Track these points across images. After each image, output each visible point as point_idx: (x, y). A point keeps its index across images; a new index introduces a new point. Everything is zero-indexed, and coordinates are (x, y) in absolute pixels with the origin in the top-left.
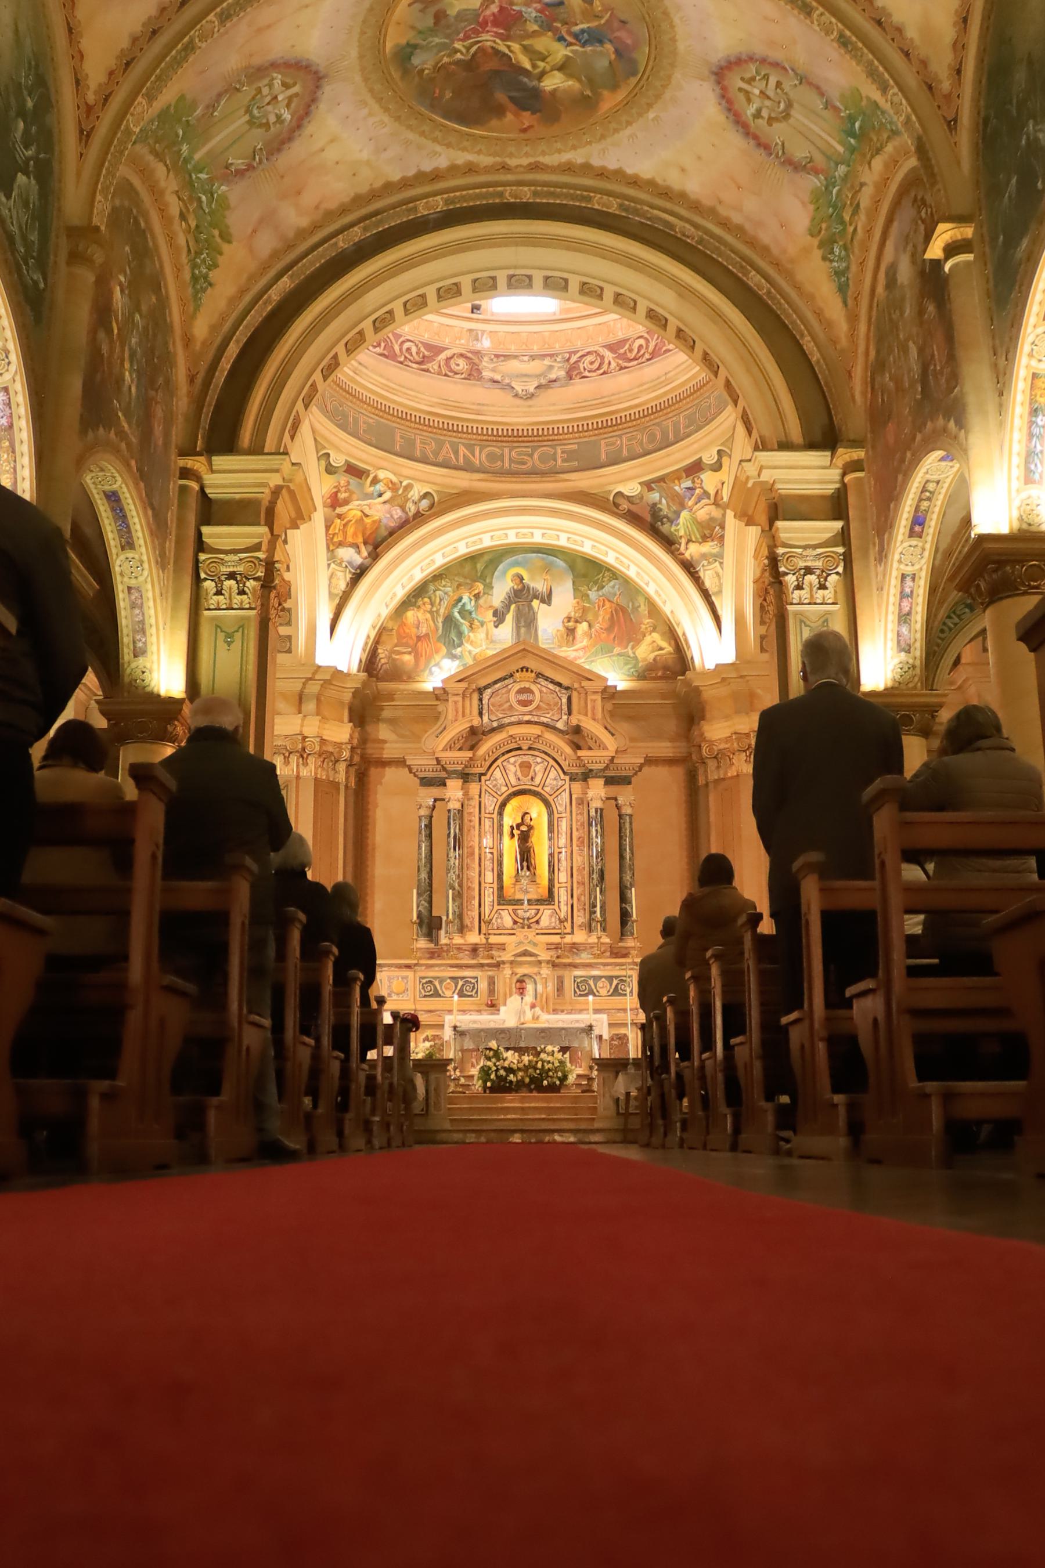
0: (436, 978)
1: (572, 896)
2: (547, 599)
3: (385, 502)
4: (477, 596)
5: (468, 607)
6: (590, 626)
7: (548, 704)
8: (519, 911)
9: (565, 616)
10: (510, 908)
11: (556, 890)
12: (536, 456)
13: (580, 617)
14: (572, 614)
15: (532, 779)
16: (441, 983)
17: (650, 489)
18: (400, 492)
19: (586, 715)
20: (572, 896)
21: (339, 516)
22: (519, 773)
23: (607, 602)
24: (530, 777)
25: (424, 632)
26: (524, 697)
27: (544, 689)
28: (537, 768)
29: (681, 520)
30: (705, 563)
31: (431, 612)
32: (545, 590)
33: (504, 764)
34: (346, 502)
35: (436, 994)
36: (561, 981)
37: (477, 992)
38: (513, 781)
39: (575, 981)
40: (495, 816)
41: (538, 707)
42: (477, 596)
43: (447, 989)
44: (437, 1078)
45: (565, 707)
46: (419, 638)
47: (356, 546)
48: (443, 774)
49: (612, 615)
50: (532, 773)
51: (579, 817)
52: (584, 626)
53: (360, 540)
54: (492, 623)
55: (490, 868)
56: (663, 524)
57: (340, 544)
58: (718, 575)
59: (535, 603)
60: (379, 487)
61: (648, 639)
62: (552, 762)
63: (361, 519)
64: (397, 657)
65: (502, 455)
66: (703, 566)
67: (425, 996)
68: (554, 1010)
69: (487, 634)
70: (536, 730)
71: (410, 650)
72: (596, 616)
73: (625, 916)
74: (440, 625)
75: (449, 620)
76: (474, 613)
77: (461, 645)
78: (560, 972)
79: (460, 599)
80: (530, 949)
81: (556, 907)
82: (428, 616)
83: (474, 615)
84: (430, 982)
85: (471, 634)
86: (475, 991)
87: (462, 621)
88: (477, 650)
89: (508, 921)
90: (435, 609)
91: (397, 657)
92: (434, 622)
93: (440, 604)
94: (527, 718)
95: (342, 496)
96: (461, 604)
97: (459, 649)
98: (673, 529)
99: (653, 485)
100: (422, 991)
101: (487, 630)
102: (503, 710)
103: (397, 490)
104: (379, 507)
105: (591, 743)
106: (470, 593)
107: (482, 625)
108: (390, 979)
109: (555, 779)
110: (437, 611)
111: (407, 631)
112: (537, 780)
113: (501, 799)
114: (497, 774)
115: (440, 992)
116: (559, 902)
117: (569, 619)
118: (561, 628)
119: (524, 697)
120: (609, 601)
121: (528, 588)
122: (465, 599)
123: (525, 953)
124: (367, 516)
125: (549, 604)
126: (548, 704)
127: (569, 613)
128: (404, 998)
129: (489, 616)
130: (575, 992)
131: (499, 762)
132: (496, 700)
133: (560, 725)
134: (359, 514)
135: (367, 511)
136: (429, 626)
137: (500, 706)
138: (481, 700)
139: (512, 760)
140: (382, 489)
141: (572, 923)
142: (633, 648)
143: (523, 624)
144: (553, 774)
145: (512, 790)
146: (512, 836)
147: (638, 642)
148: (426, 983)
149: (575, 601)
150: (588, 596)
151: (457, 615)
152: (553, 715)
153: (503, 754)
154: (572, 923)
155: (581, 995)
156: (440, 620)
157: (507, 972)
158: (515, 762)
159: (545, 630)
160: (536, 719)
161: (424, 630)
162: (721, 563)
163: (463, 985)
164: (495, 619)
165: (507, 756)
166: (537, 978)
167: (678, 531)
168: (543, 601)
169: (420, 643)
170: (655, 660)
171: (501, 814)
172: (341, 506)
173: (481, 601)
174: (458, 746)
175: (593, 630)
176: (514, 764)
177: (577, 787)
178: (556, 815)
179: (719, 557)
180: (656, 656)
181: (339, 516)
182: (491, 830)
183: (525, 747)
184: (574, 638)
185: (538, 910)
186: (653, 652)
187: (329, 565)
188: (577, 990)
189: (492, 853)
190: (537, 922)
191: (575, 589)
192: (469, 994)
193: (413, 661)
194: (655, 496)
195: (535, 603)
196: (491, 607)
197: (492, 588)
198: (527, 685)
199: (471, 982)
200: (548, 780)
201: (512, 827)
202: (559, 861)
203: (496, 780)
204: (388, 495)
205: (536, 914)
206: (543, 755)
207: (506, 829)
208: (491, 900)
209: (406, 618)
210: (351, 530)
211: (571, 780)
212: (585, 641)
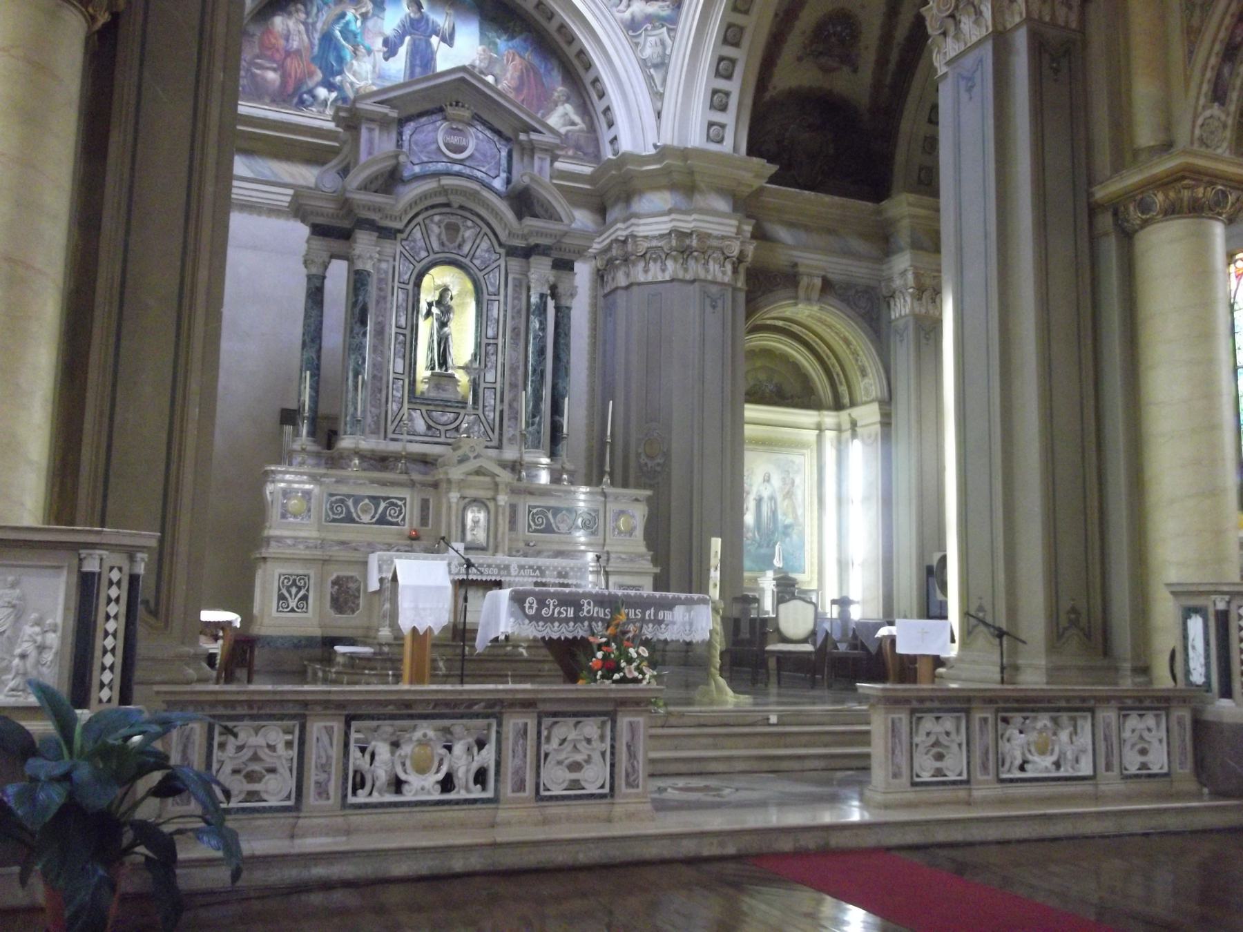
0: (349, 496)
1: (502, 401)
2: (449, 39)
4: (365, 17)
7: (485, 155)
8: (434, 413)
10: (424, 408)
11: (481, 391)
13: (487, 68)
14: (477, 63)
15: (460, 246)
16: (356, 503)
20: (502, 401)
22: (444, 237)
23: (517, 57)
24: (457, 244)
25: (295, 46)
27: (480, 135)
28: (468, 234)
30: (649, 26)
31: (305, 24)
32: (446, 26)
33: (427, 221)
35: (350, 519)
36: (513, 508)
37: (404, 519)
38: (436, 245)
39: (530, 512)
40: (410, 287)
41: (471, 157)
42: (365, 17)
43: (365, 511)
44: (631, 724)
45: (504, 162)
46: (288, 53)
48: (346, 224)
49: (522, 72)
50: (459, 239)
51: (516, 302)
54: (381, 54)
55: (401, 354)
58: (663, 43)
59: (435, 40)
61: (560, 110)
62: (486, 229)
64: (258, 72)
66: (646, 30)
67: (334, 520)
68: (510, 549)
71: (275, 66)
72: (505, 70)
73: (556, 429)
74: (316, 42)
75: (327, 38)
76: (359, 37)
77: (341, 72)
78: (515, 500)
79: (343, 15)
82: (302, 27)
83: (359, 39)
84: (342, 501)
85: (355, 62)
86: (401, 517)
87: (344, 42)
88: (362, 84)
89: (420, 425)
90: (310, 20)
91: (258, 72)
92: (308, 36)
93: (317, 15)
94: (457, 168)
96: (344, 21)
97: (338, 78)
100: (330, 513)
101: (375, 59)
102: (428, 152)
105: (538, 209)
106: (356, 10)
109: (488, 251)
110: (314, 24)
111: (273, 41)
112: (466, 248)
113: (419, 266)
114: (417, 234)
115: (354, 515)
116: (484, 407)
119: (455, 140)
120: (521, 57)
121: (427, 20)
122: (350, 15)
123: (479, 472)
125: (451, 45)
127: (474, 61)
128: (305, 521)
129: (378, 44)
130: (529, 526)
132: (419, 137)
136: (301, 40)
137: (425, 146)
138: (400, 134)
139: (437, 218)
141: (501, 434)
143: (418, 62)
145: (432, 257)
147: (549, 111)
148: (336, 502)
149: (480, 48)
150: (495, 44)
151: (338, 33)
152: (489, 169)
153: (427, 209)
154: (501, 434)
156: (317, 36)
157: (454, 496)
158: (440, 221)
160: (467, 171)
161: (295, 44)
162: (669, 30)
163: (386, 508)
164: (385, 49)
165: (431, 212)
166: (491, 505)
168: (443, 39)
169: (289, 60)
171: (418, 285)
173: (370, 24)
174: (374, 187)
176: (439, 224)
177: (515, 264)
179: (671, 22)
180: (568, 132)
182: (404, 305)
183: (456, 205)
185: (459, 414)
186: (565, 125)
188: (532, 523)
189: (404, 335)
192: (394, 520)
193: (278, 82)
195: (435, 40)
196: (381, 33)
197: (384, 10)
199: (396, 505)
200: (479, 250)
202: (486, 353)
203: (414, 241)
205: (456, 420)
206: (475, 218)
207: (423, 307)
208: (399, 395)
209: (272, 24)
211: (508, 254)
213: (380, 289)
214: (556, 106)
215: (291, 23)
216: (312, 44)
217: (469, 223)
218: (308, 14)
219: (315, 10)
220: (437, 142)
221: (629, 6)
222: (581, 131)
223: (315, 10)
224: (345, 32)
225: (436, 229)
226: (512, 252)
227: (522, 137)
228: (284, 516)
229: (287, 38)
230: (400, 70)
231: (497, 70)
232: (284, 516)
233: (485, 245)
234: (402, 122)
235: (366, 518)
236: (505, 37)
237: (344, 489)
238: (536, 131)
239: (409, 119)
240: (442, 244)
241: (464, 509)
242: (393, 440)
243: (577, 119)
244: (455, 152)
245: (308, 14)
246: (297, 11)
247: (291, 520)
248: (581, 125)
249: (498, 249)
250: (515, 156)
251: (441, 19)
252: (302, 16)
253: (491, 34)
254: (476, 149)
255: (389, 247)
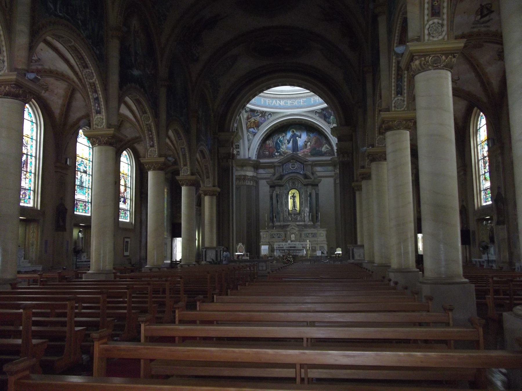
0: (273, 234)
2: (300, 137)
3: (260, 117)
4: (283, 137)
5: (281, 139)
6: (311, 143)
9: (304, 141)
12: (296, 102)
14: (306, 140)
15: (295, 185)
17: (324, 111)
18: (263, 114)
19: (307, 171)
21: (249, 122)
26: (293, 166)
27: (298, 164)
28: (296, 183)
29: (331, 118)
34: (251, 118)
35: (273, 237)
36: (301, 235)
41: (296, 168)
42: (283, 137)
45: (302, 168)
46: (270, 148)
47: (253, 128)
49: (316, 140)
52: (309, 143)
53: (254, 126)
56: (327, 119)
57: (250, 128)
59: (297, 138)
60: (258, 114)
61: (325, 146)
63: (255, 121)
65: (288, 102)
69: (286, 146)
70: (295, 175)
71: (267, 151)
72: (312, 141)
73: (317, 217)
74: (275, 144)
75: (277, 143)
79: (279, 138)
80: (294, 227)
81: (301, 215)
88: (284, 150)
89: (290, 219)
94: (294, 171)
95: (250, 117)
97: (279, 150)
98: (329, 120)
99: (324, 110)
103: (263, 114)
104: (258, 118)
107: (285, 144)
108: (263, 234)
110: (274, 141)
112: (296, 186)
117: (305, 142)
118: (304, 144)
119: (293, 166)
121: (296, 134)
122: (280, 138)
124: (256, 120)
126: (298, 168)
129: (286, 141)
131: (287, 182)
133: (301, 172)
134: (254, 120)
135: (256, 119)
136: (272, 145)
138: (283, 167)
139: (290, 181)
140: (259, 114)
142: (321, 148)
144: (300, 184)
146: (291, 199)
147: (322, 147)
149: (307, 137)
150: (310, 135)
155: (305, 237)
156: (275, 143)
159: (300, 145)
161: (271, 146)
165: (289, 180)
167: (330, 121)
168: (299, 137)
170: (326, 151)
172: (249, 119)
173: (284, 138)
175: (311, 144)
176: (291, 182)
177: (305, 187)
178: (301, 194)
181: (249, 122)
184: (307, 147)
186: (326, 149)
187: (247, 133)
190: (297, 219)
191: (307, 134)
193: (268, 154)
194: (325, 112)
195: (297, 138)
197: (287, 134)
198: (294, 163)
201: (291, 197)
203: (287, 186)
204: (260, 115)
210: (252, 124)
212: (309, 147)
213: (281, 196)
214: (324, 145)
215: (270, 142)
216: (274, 145)
217: (297, 181)
218: (273, 139)
219: (274, 138)
220: (289, 167)
221: (333, 125)
222: (330, 149)
223: (274, 138)
224: (280, 141)
225: (291, 183)
226: (305, 185)
227: (305, 163)
228: (263, 238)
229: (269, 144)
230: (291, 146)
231: (310, 141)
232: (263, 238)
233: (300, 184)
234: (283, 165)
235: (276, 237)
236: (312, 134)
237: (272, 233)
238: (308, 162)
239: (285, 163)
240: (292, 185)
241: (291, 235)
242: (285, 222)
243: (329, 147)
244: (293, 168)
245: (273, 139)
246: (271, 139)
247: (264, 238)
248: (330, 148)
249: (302, 185)
250: (305, 167)
251: (298, 133)
252: (272, 140)
253: (309, 134)
254: (297, 167)
255: (282, 188)
